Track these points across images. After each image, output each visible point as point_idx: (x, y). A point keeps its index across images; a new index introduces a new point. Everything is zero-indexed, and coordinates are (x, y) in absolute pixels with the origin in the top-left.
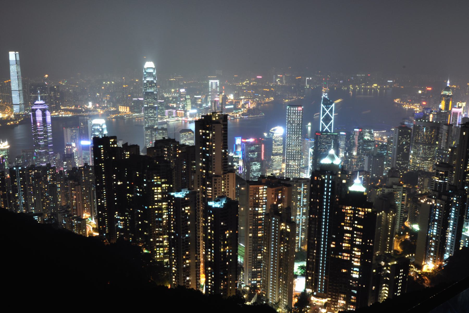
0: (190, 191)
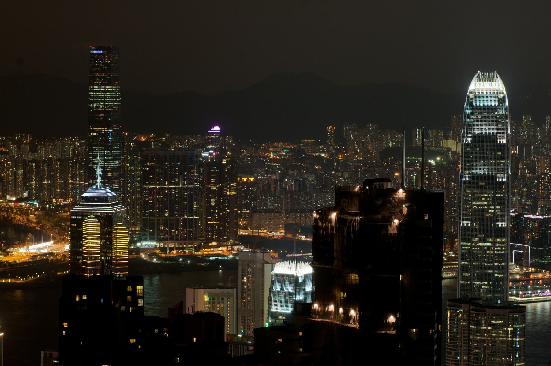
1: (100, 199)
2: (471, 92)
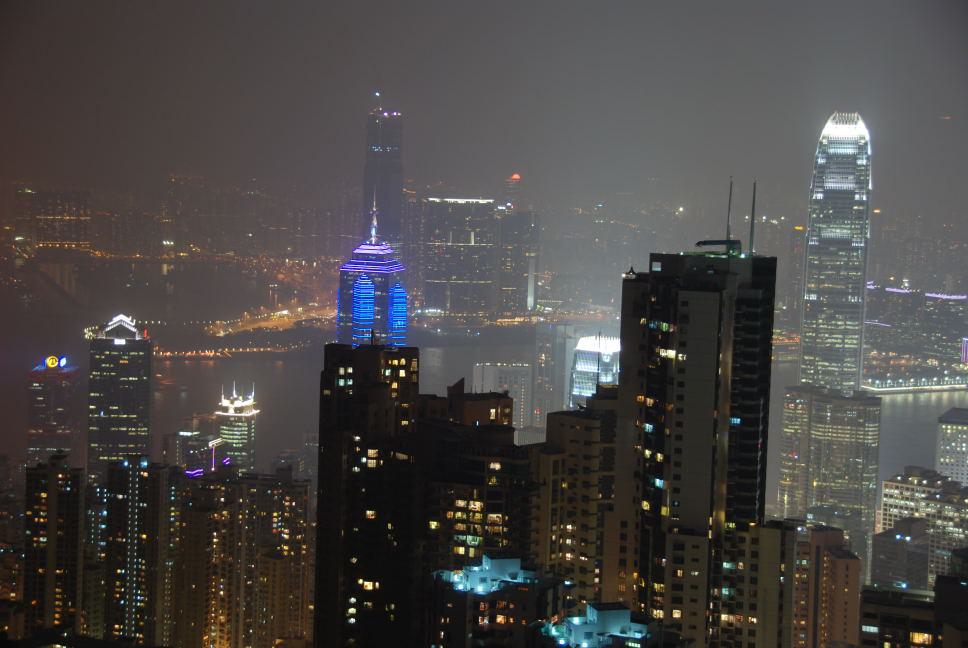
0: (531, 574)
1: (379, 257)
2: (824, 138)
